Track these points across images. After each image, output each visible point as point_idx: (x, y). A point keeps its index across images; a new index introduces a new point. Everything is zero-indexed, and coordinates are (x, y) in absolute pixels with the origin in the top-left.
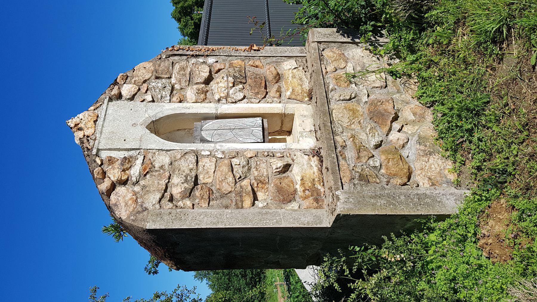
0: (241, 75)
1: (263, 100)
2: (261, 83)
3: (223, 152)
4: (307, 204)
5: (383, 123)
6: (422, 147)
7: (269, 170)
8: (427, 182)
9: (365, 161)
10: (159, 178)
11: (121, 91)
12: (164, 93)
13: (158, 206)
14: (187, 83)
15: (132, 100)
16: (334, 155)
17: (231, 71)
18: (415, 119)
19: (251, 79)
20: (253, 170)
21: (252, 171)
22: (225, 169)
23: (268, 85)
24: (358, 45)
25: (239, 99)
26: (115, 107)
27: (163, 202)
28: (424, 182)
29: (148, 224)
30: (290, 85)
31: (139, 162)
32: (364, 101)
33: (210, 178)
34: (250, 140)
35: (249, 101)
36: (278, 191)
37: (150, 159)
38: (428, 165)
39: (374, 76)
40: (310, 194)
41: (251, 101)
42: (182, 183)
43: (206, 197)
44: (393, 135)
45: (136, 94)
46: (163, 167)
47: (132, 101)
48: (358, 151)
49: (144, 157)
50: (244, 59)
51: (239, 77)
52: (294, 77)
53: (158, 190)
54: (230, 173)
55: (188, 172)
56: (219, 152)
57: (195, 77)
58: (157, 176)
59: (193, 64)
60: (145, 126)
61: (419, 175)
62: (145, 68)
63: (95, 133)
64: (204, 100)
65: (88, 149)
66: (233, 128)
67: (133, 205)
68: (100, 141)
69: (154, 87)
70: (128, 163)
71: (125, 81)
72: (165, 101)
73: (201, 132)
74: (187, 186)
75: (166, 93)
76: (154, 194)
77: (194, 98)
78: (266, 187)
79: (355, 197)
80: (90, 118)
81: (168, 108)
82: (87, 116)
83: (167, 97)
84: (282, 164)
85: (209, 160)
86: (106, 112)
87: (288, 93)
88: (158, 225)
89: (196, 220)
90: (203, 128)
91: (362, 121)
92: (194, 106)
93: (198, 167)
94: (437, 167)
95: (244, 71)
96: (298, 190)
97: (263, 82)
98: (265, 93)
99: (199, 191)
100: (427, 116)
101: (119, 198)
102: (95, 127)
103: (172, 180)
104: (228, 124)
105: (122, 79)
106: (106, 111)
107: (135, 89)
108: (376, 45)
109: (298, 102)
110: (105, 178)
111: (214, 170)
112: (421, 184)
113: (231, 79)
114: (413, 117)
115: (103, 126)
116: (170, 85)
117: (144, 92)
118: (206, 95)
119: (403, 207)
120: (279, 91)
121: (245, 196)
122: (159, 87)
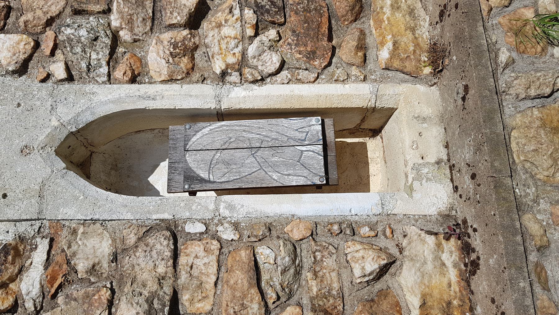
1: (326, 71)
2: (319, 26)
3: (236, 226)
10: (86, 306)
12: (94, 56)
14: (149, 23)
15: (24, 74)
19: (296, 13)
20: (307, 275)
21: (303, 276)
23: (334, 27)
25: (270, 72)
35: (292, 76)
37: (63, 251)
41: (299, 77)
46: (97, 268)
47: (24, 76)
49: (52, 240)
51: (267, 7)
54: (254, 291)
55: (155, 287)
56: (226, 225)
57: (165, 9)
58: (80, 301)
60: (54, 149)
64: (188, 73)
69: (69, 40)
70: (13, 263)
72: (98, 79)
75: (100, 57)
77: (166, 69)
83: (101, 67)
85: (202, 247)
87: (385, 54)
90: (190, 143)
93: (178, 270)
97: (325, 20)
98: (330, 54)
107: (27, 47)
111: (214, 278)
113: (249, 14)
116: (108, 32)
117: (48, 52)
118: (193, 58)
120: (362, 47)
122: (83, 39)
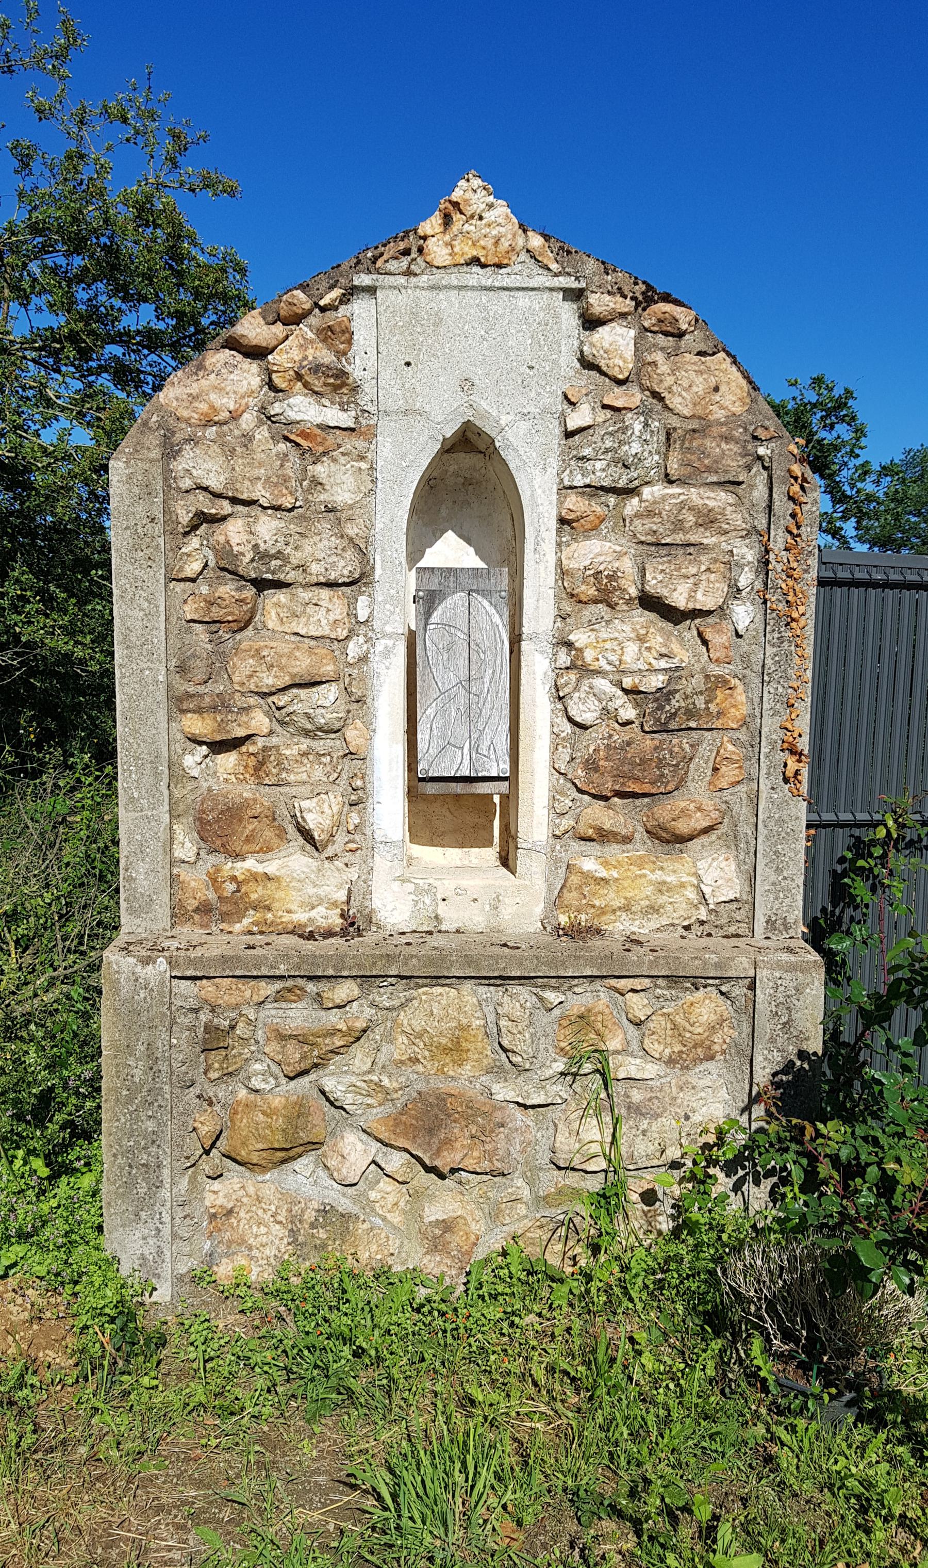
0: (675, 714)
1: (569, 785)
2: (636, 779)
3: (364, 659)
4: (193, 884)
5: (402, 1127)
6: (310, 1216)
7: (304, 790)
8: (218, 1202)
9: (267, 1050)
10: (275, 479)
11: (614, 324)
12: (599, 465)
13: (187, 483)
14: (650, 539)
15: (582, 365)
16: (282, 970)
17: (693, 681)
18: (426, 1220)
19: (656, 748)
20: (305, 744)
21: (303, 740)
22: (302, 664)
23: (638, 802)
24: (743, 1111)
25: (569, 709)
26: (542, 314)
27: (201, 496)
28: (221, 1194)
29: (121, 465)
30: (629, 874)
31: (334, 416)
32: (495, 1088)
33: (278, 623)
34: (427, 737)
35: (564, 739)
36: (229, 809)
37: (339, 446)
38: (267, 1217)
39: (598, 1137)
40: (225, 894)
41: (560, 747)
42: (256, 546)
43: (216, 613)
44: (360, 1146)
45: (605, 374)
46: (319, 488)
47: (578, 365)
48: (300, 1038)
49: (353, 430)
50: (752, 726)
51: (668, 708)
52: (662, 887)
53: (232, 481)
54: (287, 680)
55: (295, 562)
56: (365, 648)
57: (669, 562)
58: (280, 472)
59: (732, 551)
60: (472, 419)
61: (243, 1187)
62: (716, 389)
63: (434, 270)
64: (572, 596)
65: (375, 260)
66: (474, 690)
67: (196, 416)
68: (403, 291)
69: (624, 430)
70: (325, 384)
71: (656, 329)
72: (568, 472)
73: (463, 591)
74: (247, 559)
75: (598, 474)
76: (219, 470)
77: (576, 566)
78: (248, 776)
79: (151, 1005)
80: (489, 243)
81: (536, 483)
82: (494, 232)
83: (583, 475)
84: (312, 826)
85: (339, 617)
86: (518, 289)
87: (589, 865)
88: (118, 491)
89: (133, 589)
91: (420, 1068)
92: (542, 567)
93: (313, 588)
94: (259, 1239)
95: (693, 724)
96: (239, 865)
97: (647, 788)
98: (593, 791)
99: (233, 593)
100: (438, 1259)
101: (213, 375)
102: (455, 265)
103: (269, 516)
104: (489, 672)
105: (660, 321)
106: (523, 289)
107: (617, 369)
108: (741, 1173)
109: (556, 892)
110: (284, 324)
111: (303, 632)
112: (216, 1185)
113: (656, 681)
114: (432, 1219)
115: (460, 288)
116: (636, 483)
117: (606, 402)
118: (596, 602)
119: (123, 1120)
120: (603, 836)
121: (215, 719)
122: (627, 447)
